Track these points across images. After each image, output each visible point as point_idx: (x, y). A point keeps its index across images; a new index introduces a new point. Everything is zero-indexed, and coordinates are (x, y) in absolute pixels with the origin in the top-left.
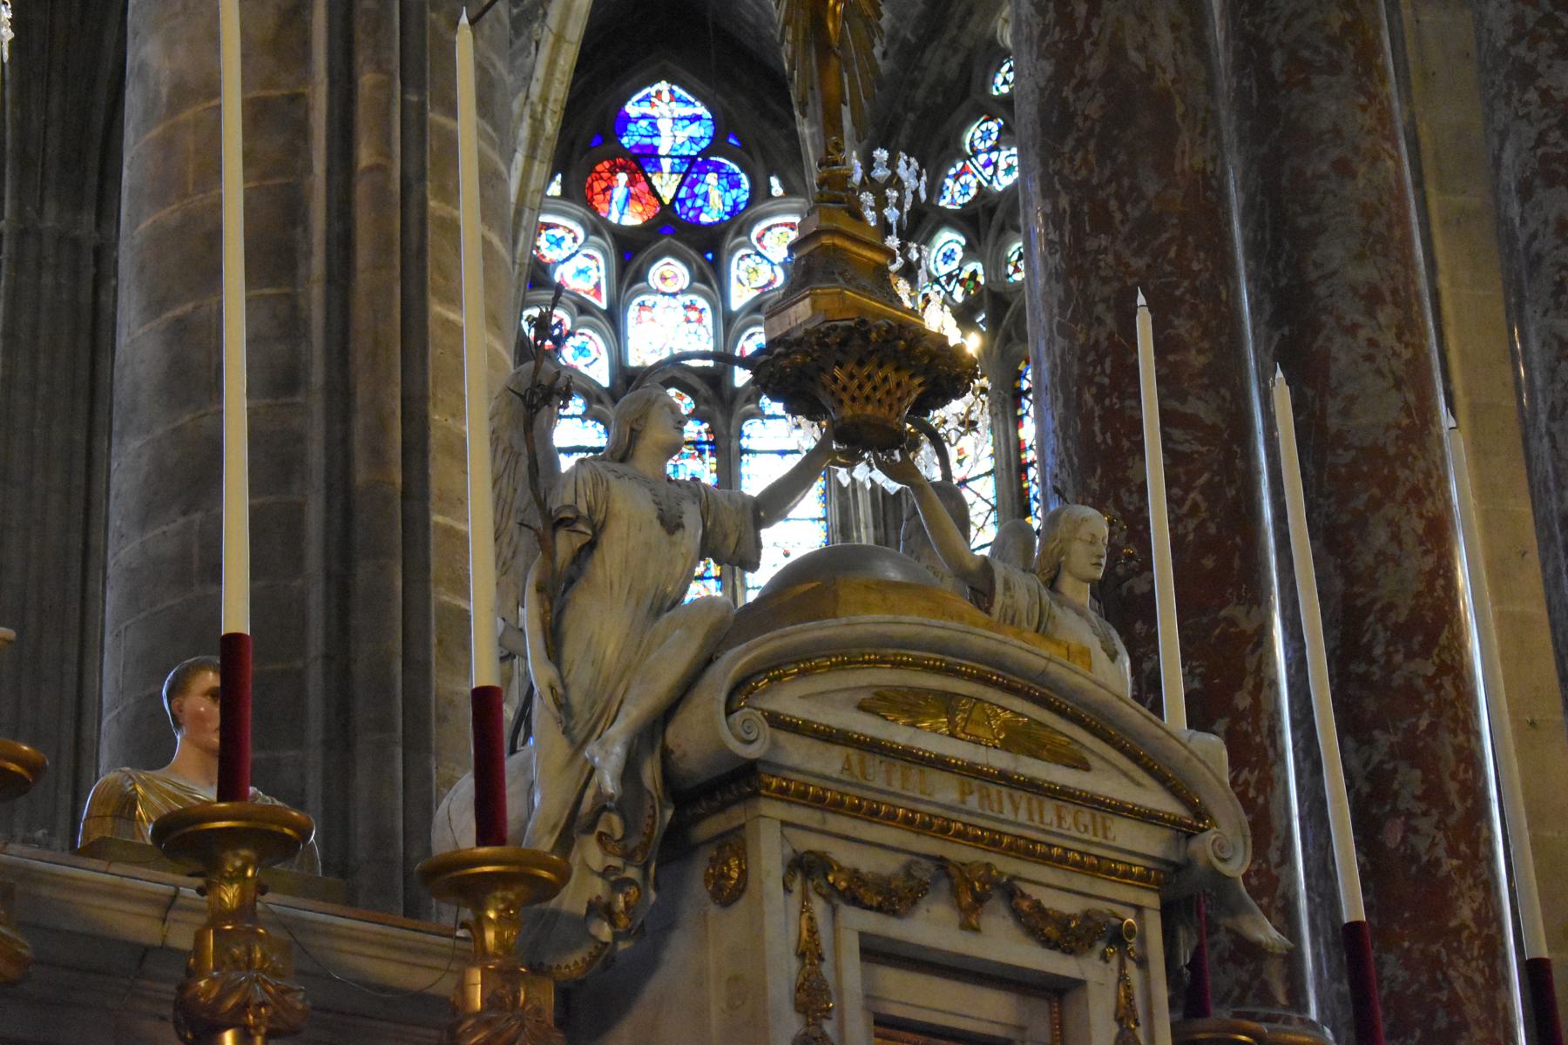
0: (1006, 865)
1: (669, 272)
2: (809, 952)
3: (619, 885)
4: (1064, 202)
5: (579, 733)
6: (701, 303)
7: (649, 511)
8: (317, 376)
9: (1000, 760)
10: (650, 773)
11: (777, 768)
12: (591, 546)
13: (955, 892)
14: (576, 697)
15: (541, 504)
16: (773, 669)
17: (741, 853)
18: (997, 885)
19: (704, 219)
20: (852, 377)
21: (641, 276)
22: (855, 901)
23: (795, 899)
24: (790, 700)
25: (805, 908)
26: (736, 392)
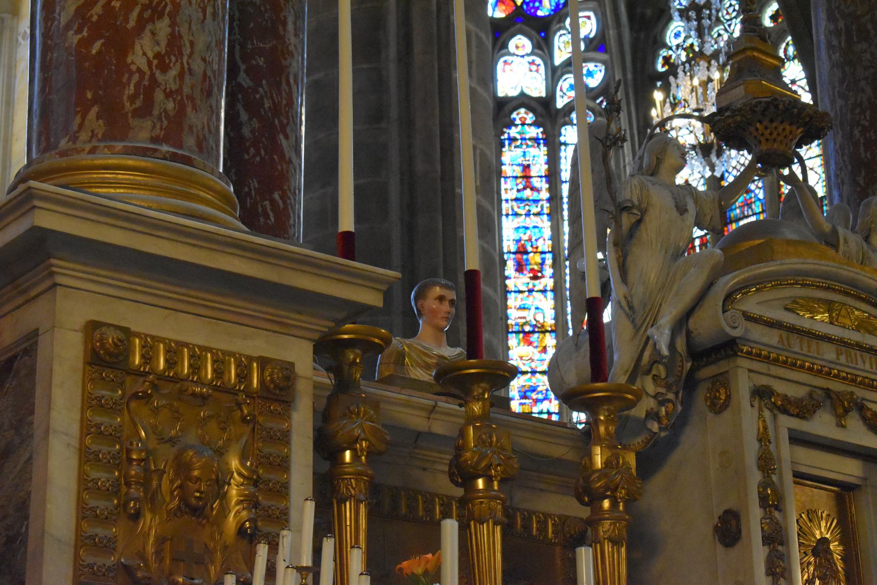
0: (860, 393)
1: (520, 43)
2: (763, 438)
3: (661, 403)
4: (841, 24)
5: (638, 321)
6: (538, 61)
7: (670, 203)
8: (394, 112)
9: (855, 337)
10: (681, 344)
11: (745, 340)
12: (639, 222)
13: (834, 408)
14: (636, 303)
15: (613, 199)
16: (743, 288)
17: (726, 386)
18: (856, 404)
19: (540, 13)
20: (766, 128)
21: (505, 46)
22: (785, 411)
23: (755, 411)
24: (752, 304)
25: (760, 416)
26: (558, 111)
